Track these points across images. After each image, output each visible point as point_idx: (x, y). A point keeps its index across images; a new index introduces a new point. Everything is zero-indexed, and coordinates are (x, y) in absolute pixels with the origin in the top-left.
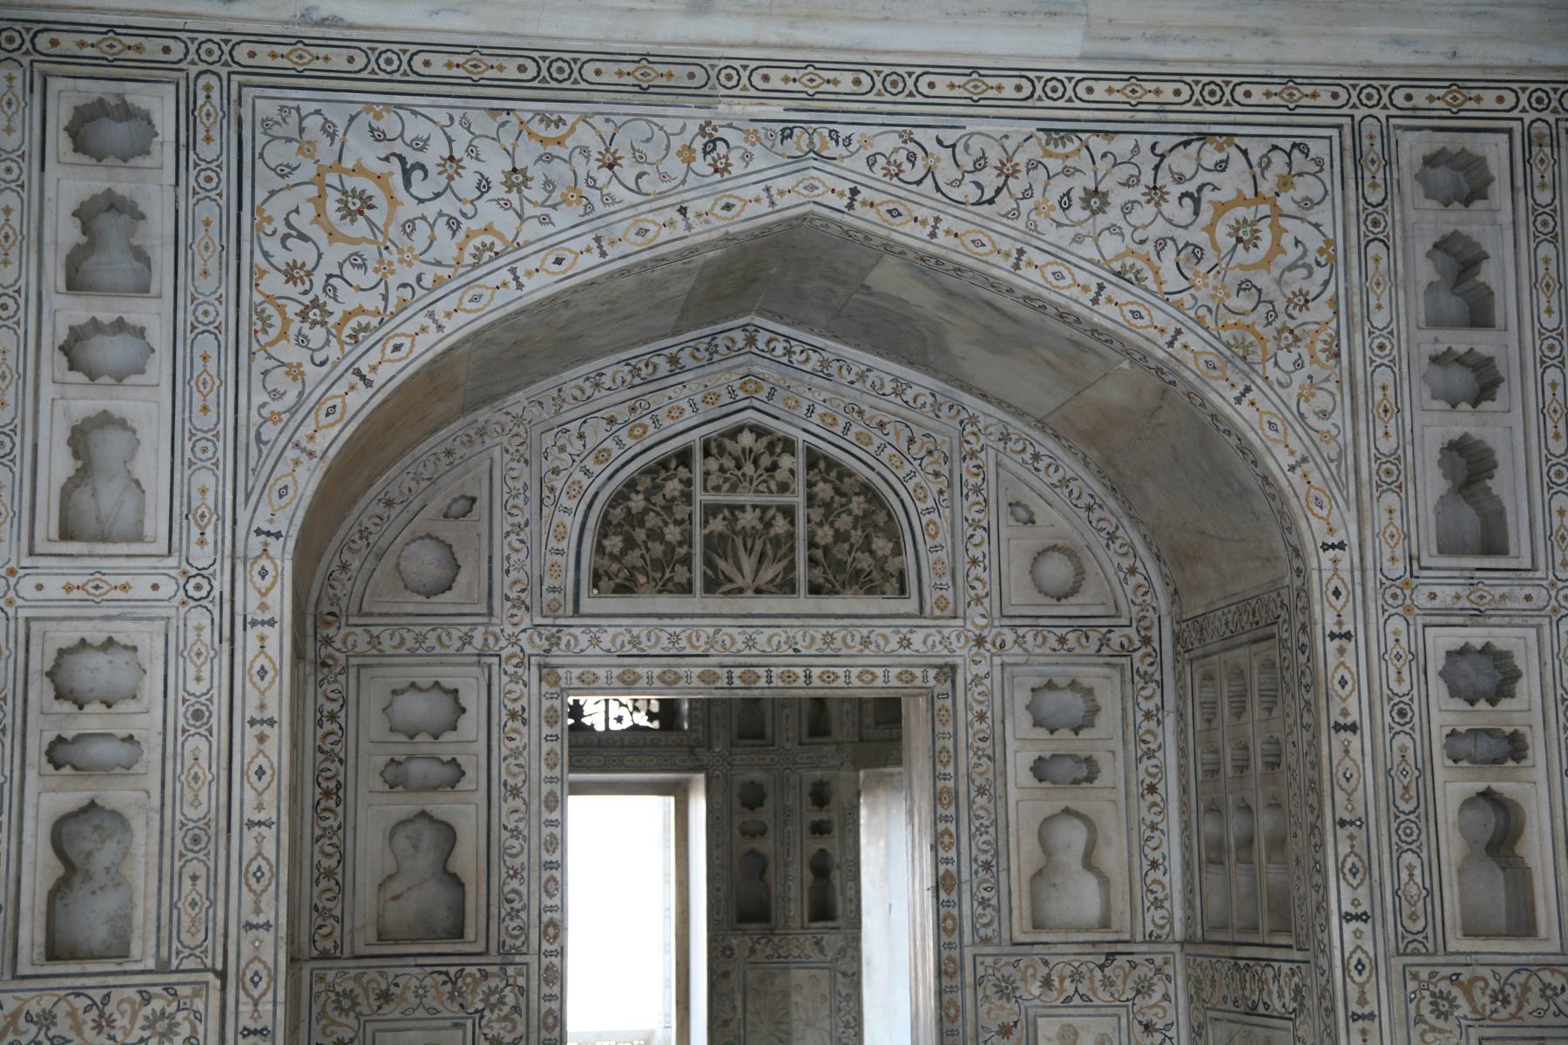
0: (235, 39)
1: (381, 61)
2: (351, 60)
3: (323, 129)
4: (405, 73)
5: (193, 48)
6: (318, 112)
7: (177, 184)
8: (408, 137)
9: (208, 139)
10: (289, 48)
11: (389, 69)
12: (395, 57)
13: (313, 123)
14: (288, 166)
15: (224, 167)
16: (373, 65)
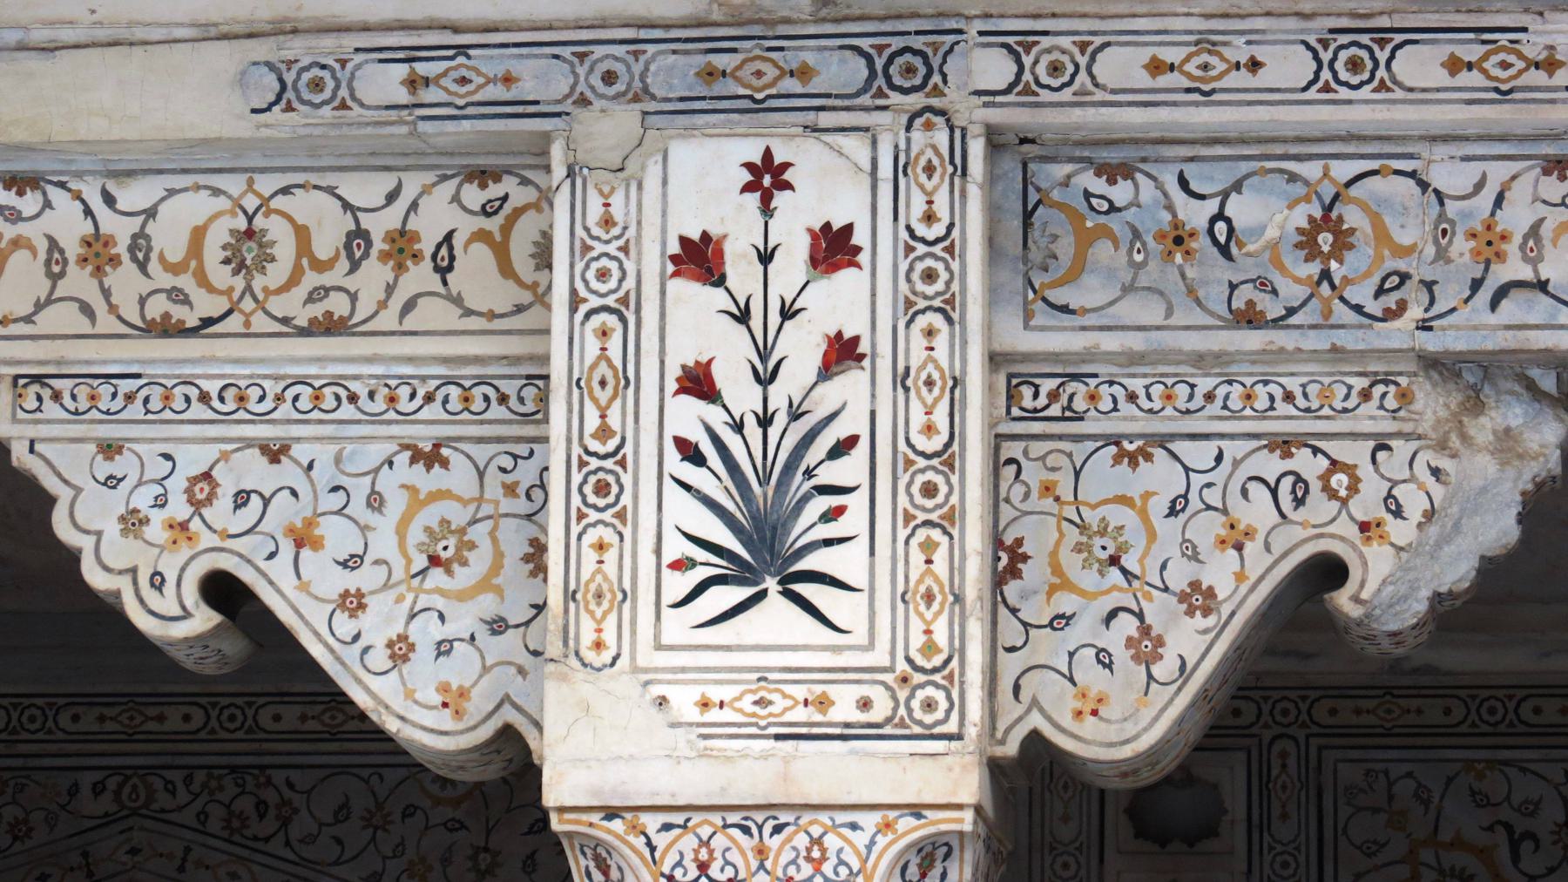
0: (1313, 694)
1: (1483, 711)
2: (1447, 712)
3: (1416, 795)
4: (1511, 724)
5: (1266, 708)
6: (1409, 775)
7: (1250, 871)
8: (1517, 799)
9: (1284, 816)
10: (1375, 702)
11: (1492, 720)
12: (1499, 705)
13: (1404, 788)
14: (1375, 842)
15: (1303, 849)
16: (1473, 716)
